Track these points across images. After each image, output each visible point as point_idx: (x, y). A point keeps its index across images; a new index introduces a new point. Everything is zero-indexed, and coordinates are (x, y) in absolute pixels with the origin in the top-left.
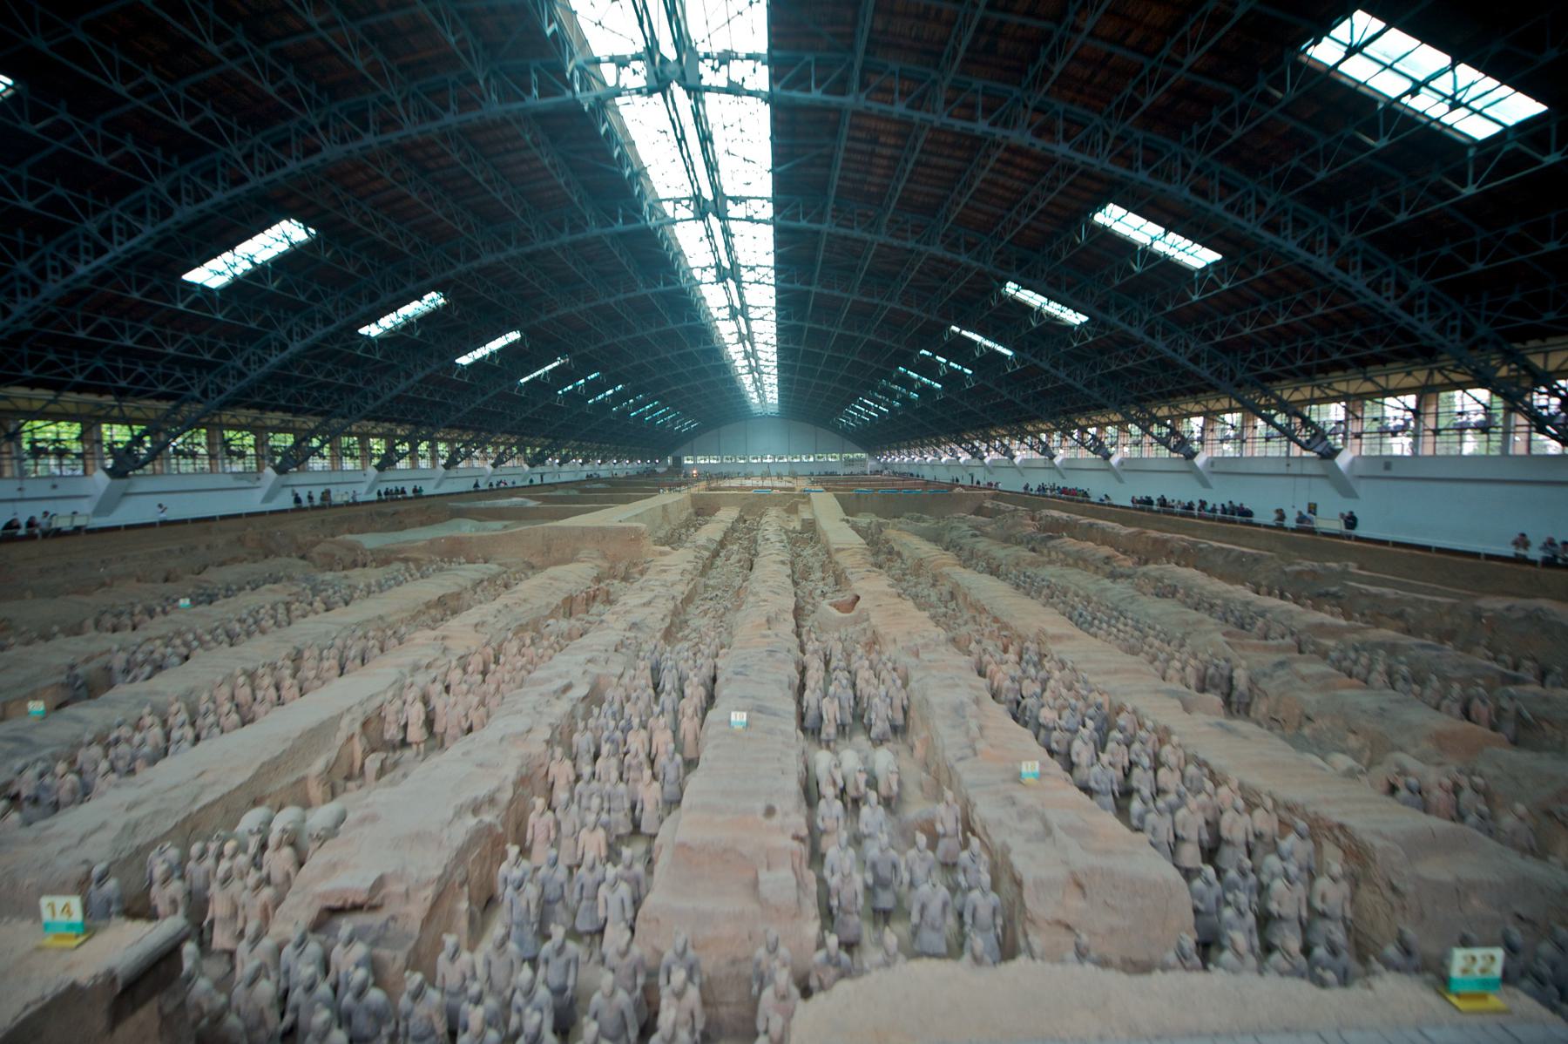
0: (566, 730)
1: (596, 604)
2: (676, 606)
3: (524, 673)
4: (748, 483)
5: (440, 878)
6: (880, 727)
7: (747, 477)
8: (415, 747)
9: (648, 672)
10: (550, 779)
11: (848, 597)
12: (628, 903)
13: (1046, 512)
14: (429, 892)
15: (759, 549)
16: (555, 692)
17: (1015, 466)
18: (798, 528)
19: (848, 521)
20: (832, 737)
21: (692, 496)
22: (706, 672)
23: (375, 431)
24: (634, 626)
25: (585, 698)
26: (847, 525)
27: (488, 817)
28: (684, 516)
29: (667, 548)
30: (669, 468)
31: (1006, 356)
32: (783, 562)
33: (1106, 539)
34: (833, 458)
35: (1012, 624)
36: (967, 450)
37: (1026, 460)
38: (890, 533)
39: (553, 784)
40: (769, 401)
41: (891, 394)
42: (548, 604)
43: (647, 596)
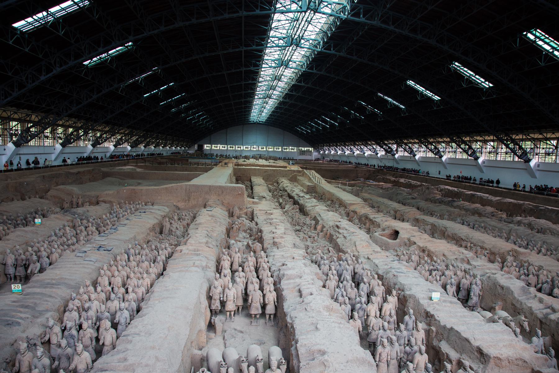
6: (474, 299)
7: (246, 157)
8: (228, 313)
11: (387, 232)
13: (442, 187)
15: (301, 202)
17: (415, 160)
19: (338, 187)
23: (68, 124)
26: (339, 190)
30: (196, 151)
31: (434, 100)
32: (328, 211)
33: (484, 202)
34: (291, 150)
35: (485, 246)
36: (386, 150)
37: (450, 159)
38: (366, 195)
40: (264, 114)
41: (346, 115)
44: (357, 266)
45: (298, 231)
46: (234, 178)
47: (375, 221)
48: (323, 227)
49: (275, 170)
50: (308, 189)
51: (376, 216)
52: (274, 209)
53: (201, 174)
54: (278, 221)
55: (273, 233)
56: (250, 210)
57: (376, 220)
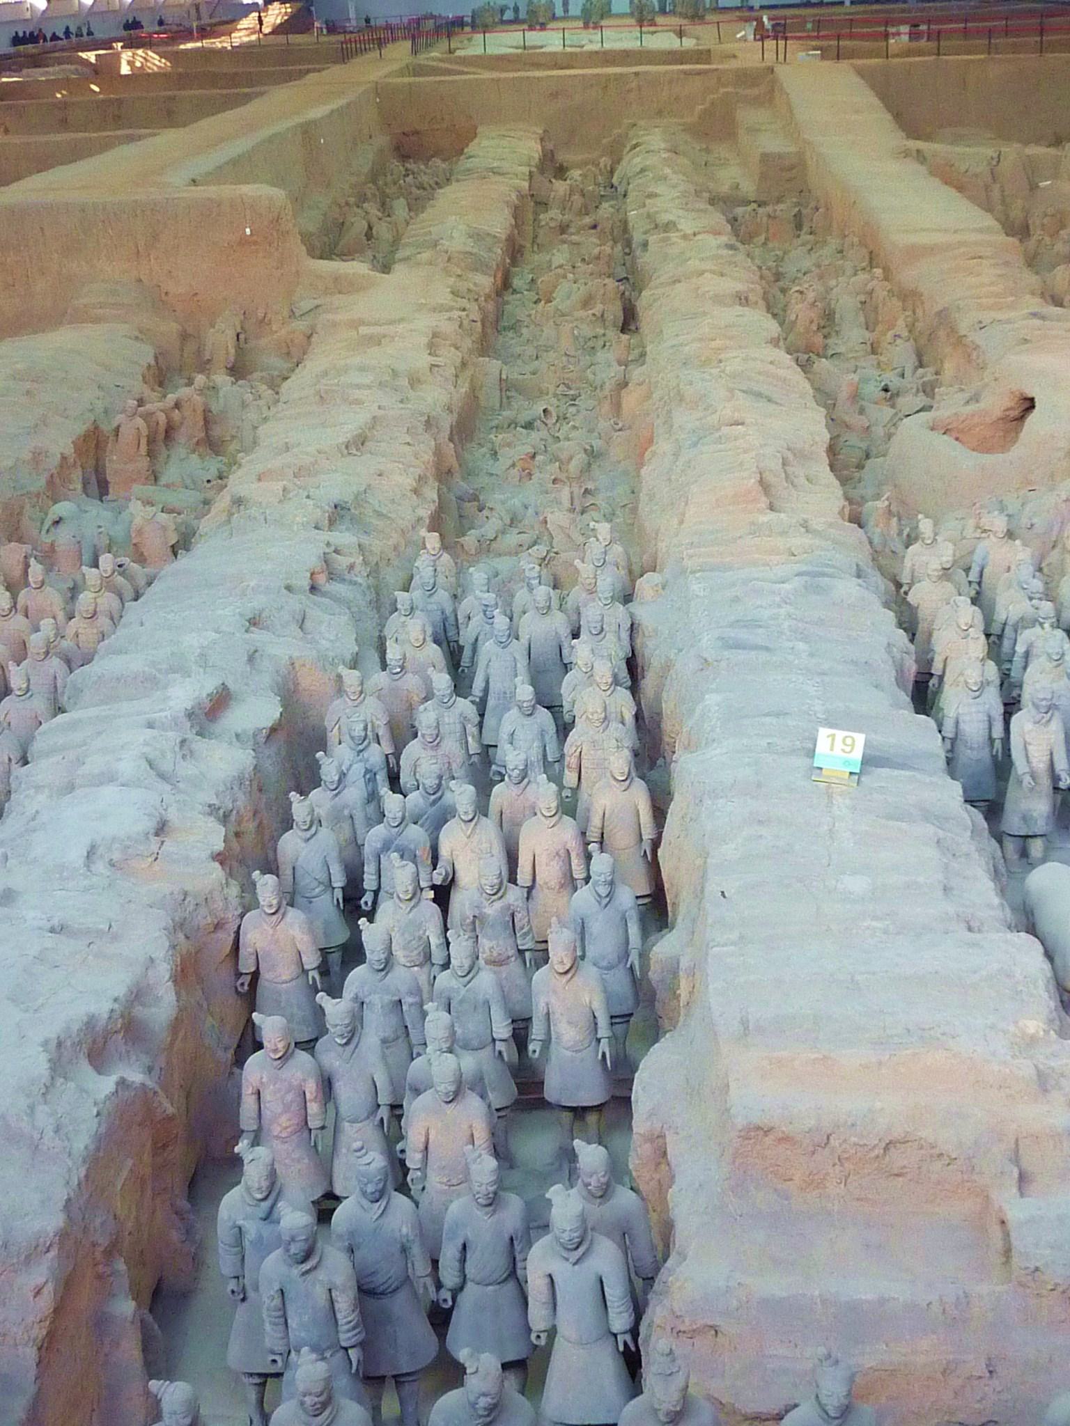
0: (250, 826)
1: (179, 451)
2: (438, 453)
3: (55, 664)
4: (550, 41)
5: (63, 1235)
9: (434, 652)
10: (247, 966)
11: (996, 403)
12: (616, 1292)
14: (41, 1273)
15: (645, 259)
16: (190, 715)
18: (748, 188)
19: (920, 157)
20: (1041, 826)
21: (379, 90)
22: (615, 648)
24: (338, 513)
25: (273, 730)
26: (923, 169)
27: (136, 1076)
28: (364, 160)
29: (357, 268)
32: (742, 299)
39: (256, 975)
42: (38, 457)
43: (351, 422)
44: (591, 615)
45: (529, 426)
46: (382, 141)
47: (977, 347)
48: (649, 396)
49: (608, 77)
50: (763, 177)
51: (987, 316)
52: (434, 310)
53: (140, 138)
54: (367, 379)
55: (287, 448)
56: (301, 325)
57: (977, 338)
